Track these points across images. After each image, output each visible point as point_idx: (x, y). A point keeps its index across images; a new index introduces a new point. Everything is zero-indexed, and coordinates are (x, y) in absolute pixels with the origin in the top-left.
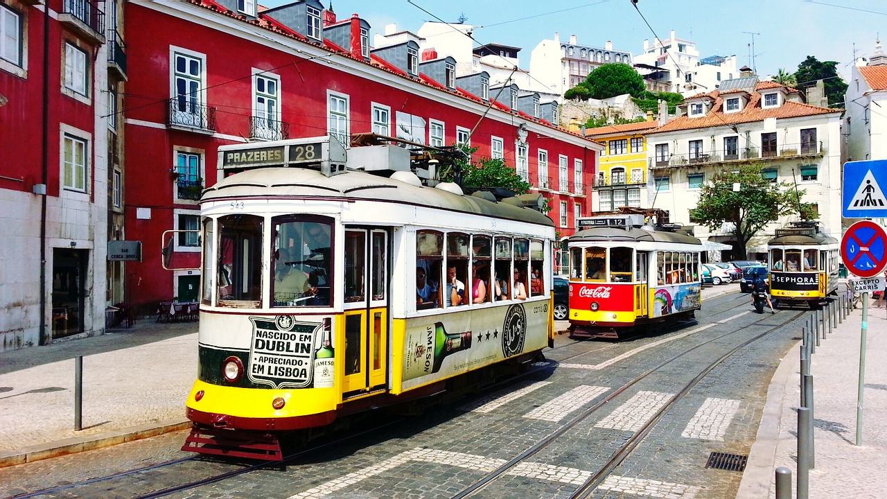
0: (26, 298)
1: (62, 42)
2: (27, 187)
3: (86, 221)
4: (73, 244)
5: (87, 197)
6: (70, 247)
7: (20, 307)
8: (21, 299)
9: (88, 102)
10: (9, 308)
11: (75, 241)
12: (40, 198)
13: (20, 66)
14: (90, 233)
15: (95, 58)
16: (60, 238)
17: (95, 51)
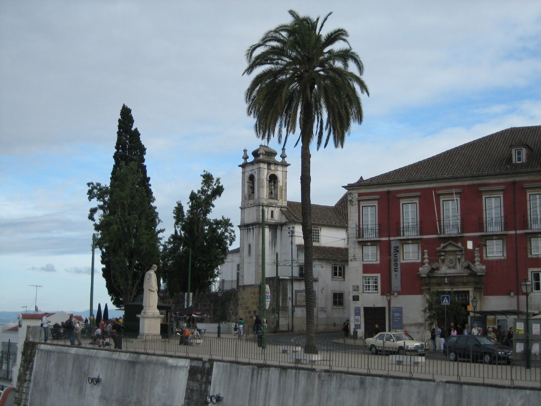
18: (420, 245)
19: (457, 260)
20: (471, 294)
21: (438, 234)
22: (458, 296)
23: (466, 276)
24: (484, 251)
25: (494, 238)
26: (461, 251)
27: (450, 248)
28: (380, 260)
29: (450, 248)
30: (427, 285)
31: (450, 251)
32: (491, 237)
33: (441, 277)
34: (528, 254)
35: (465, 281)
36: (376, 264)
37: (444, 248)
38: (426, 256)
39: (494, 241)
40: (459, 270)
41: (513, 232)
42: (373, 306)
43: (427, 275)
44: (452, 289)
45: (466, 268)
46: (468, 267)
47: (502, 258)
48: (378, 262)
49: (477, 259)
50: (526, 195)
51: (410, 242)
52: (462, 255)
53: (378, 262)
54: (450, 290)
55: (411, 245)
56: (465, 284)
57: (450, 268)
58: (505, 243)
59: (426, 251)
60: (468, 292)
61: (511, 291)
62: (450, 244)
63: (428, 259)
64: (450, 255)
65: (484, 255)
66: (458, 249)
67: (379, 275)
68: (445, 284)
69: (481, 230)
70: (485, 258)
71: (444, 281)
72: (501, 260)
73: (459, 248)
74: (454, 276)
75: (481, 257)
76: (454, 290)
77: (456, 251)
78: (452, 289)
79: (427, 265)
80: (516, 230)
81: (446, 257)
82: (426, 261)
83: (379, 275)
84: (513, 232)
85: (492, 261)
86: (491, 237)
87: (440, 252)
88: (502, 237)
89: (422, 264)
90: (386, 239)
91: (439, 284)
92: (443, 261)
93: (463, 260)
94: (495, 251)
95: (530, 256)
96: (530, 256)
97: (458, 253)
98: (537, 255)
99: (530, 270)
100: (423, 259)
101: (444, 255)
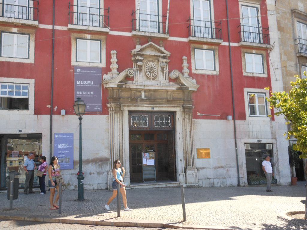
0: (226, 164)
1: (242, 54)
2: (223, 117)
3: (268, 129)
4: (258, 141)
5: (268, 119)
6: (257, 142)
7: (223, 168)
8: (223, 165)
9: (265, 76)
10: (215, 168)
11: (260, 139)
12: (232, 122)
13: (215, 70)
14: (272, 136)
15: (268, 55)
16: (249, 138)
17: (269, 52)
18: (104, 44)
19: (160, 69)
20: (179, 116)
21: (135, 30)
22: (157, 119)
23: (173, 91)
24: (193, 61)
25: (205, 47)
26: (164, 57)
27: (148, 52)
28: (36, 59)
29: (148, 52)
30: (116, 100)
31: (150, 56)
32: (200, 44)
33: (137, 90)
34: (243, 71)
35: (170, 98)
36: (28, 64)
37: (141, 50)
38: (114, 59)
39: (204, 51)
40: (161, 83)
41: (226, 44)
42: (17, 132)
43: (118, 86)
44: (153, 108)
45: (171, 80)
46: (176, 80)
47: (214, 73)
48: (32, 60)
49: (186, 70)
50: (238, 5)
51: (89, 36)
52: (166, 63)
53: (32, 60)
54: (150, 109)
55: (89, 41)
56: (170, 102)
57: (149, 78)
58: (217, 56)
59: (113, 52)
60: (173, 114)
61: (228, 115)
62: (151, 46)
63: (117, 63)
64: (150, 61)
65: (193, 68)
66: (162, 55)
67: (32, 82)
68: (143, 100)
69: (188, 35)
70: (193, 71)
71: (141, 96)
72: (213, 76)
73: (162, 52)
74: (155, 91)
75: (190, 68)
76: (156, 109)
77: (159, 56)
78: (153, 108)
79: (115, 71)
80: (229, 42)
81: (145, 61)
82: (114, 66)
83: (32, 82)
84: (226, 44)
85: (203, 76)
86: (200, 44)
87: (135, 55)
88: (213, 47)
89: (107, 69)
90: (50, 27)
91: (135, 100)
92: (140, 67)
93: (166, 71)
94: (205, 62)
95: (245, 74)
96: (245, 74)
97: (161, 60)
98: (253, 73)
99: (246, 90)
100: (109, 63)
101: (141, 61)
